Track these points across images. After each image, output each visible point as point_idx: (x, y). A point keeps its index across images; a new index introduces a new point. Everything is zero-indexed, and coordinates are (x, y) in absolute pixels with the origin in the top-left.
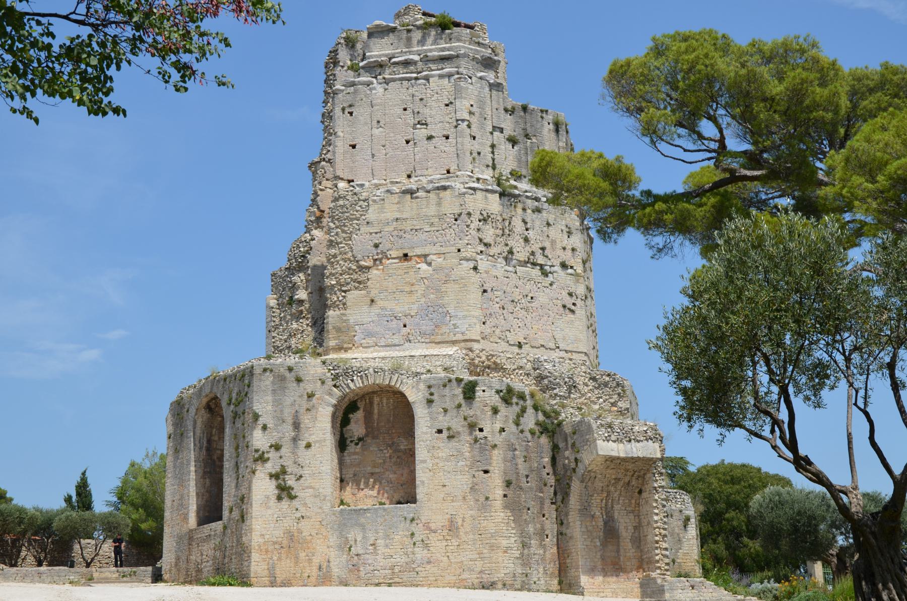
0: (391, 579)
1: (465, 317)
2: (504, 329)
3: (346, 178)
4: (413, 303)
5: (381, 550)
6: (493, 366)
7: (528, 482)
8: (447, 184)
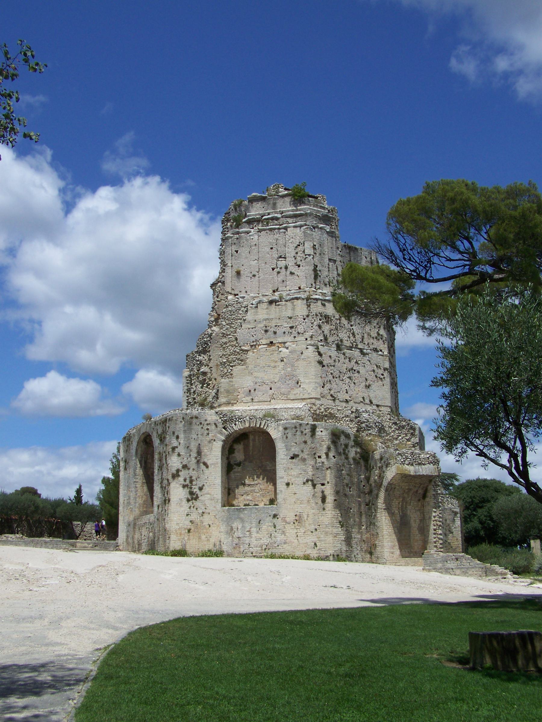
0: (260, 553)
1: (310, 383)
2: (336, 391)
3: (233, 293)
4: (277, 374)
5: (254, 535)
6: (329, 415)
7: (350, 491)
8: (298, 296)
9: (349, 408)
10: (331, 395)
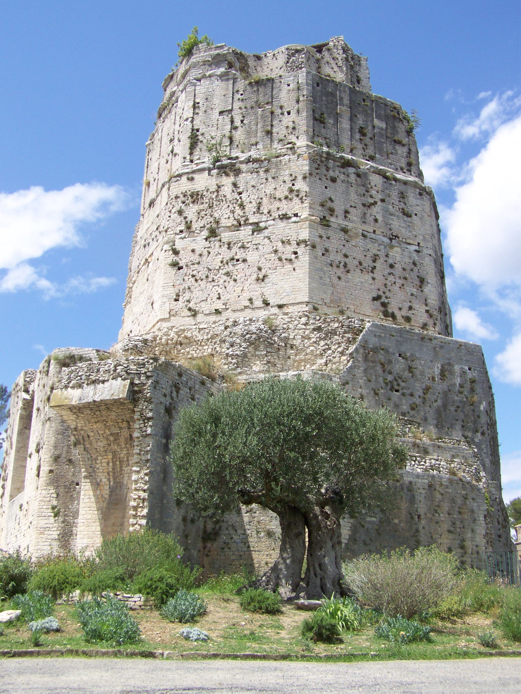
2: (199, 300)
9: (221, 322)
10: (190, 309)
